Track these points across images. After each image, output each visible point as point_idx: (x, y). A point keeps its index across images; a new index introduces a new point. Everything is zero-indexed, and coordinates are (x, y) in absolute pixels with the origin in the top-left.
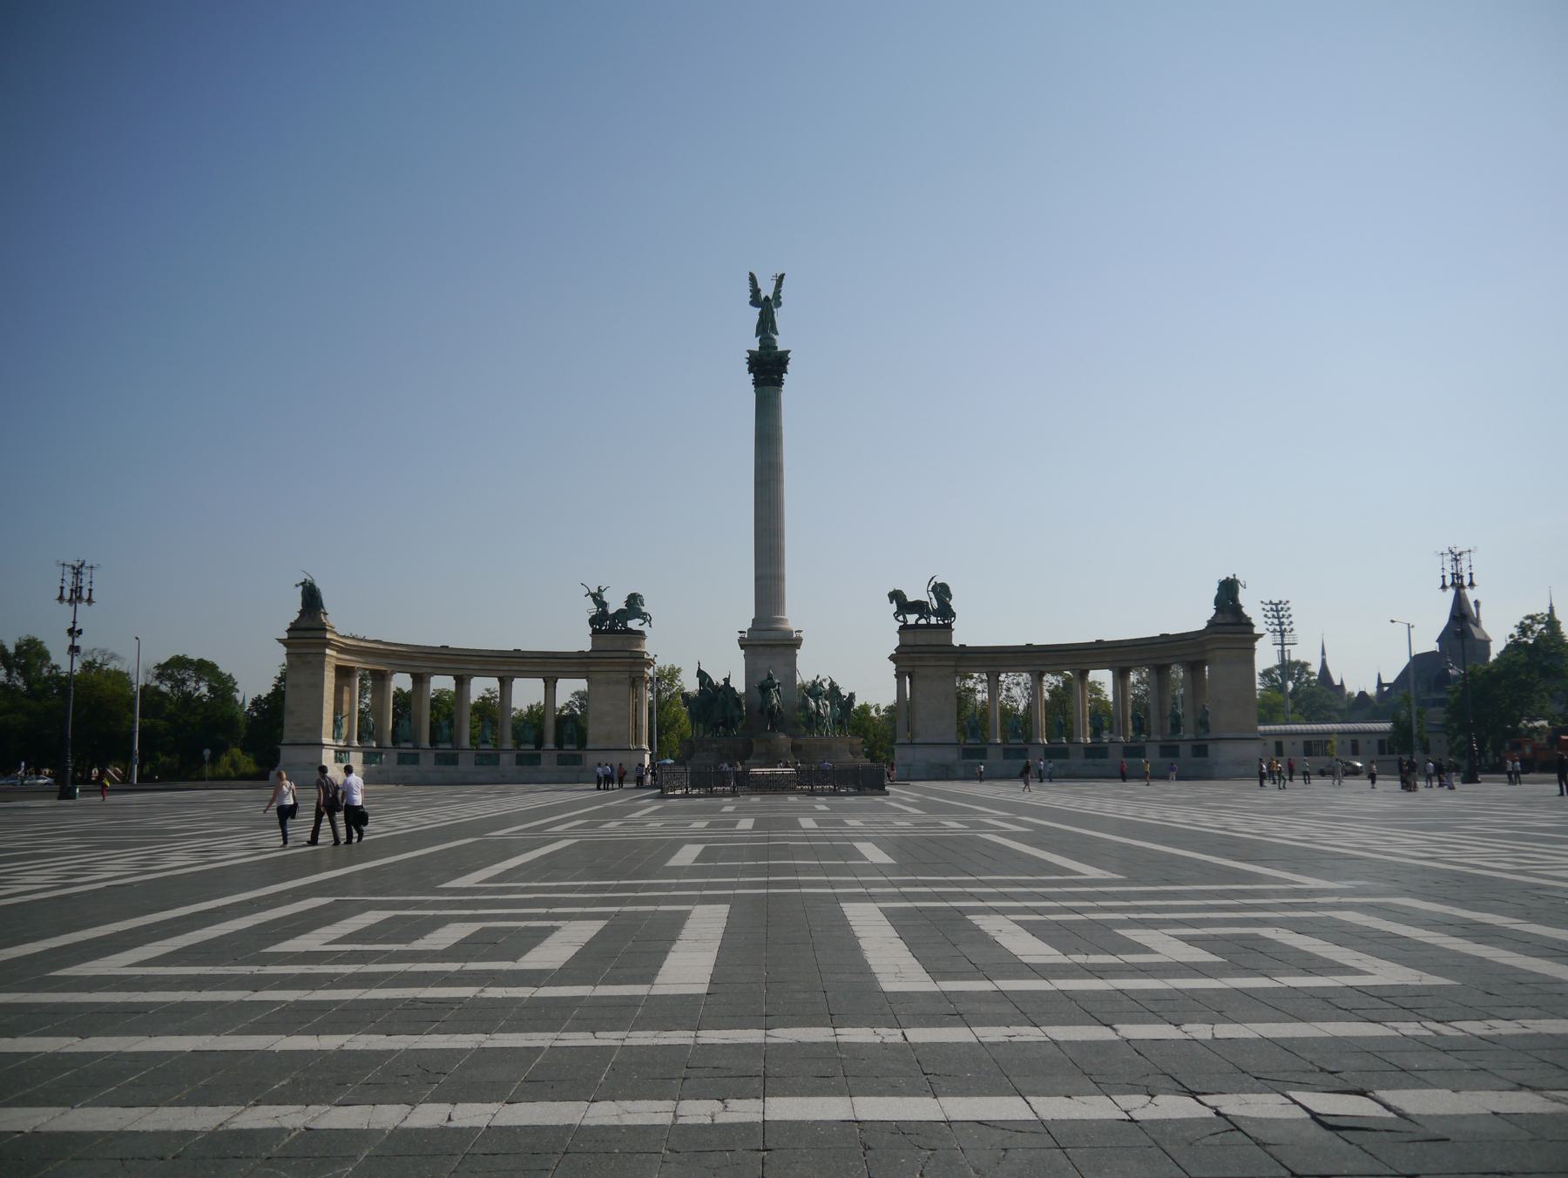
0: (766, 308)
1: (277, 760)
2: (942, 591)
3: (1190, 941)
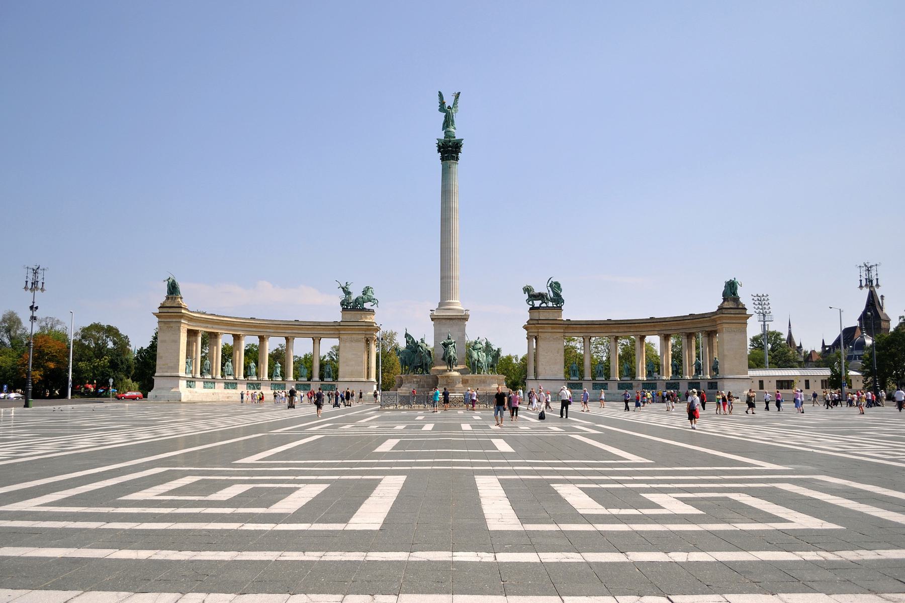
2: (555, 287)
3: (685, 501)
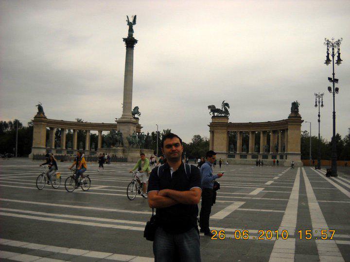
0: (131, 25)
1: (30, 152)
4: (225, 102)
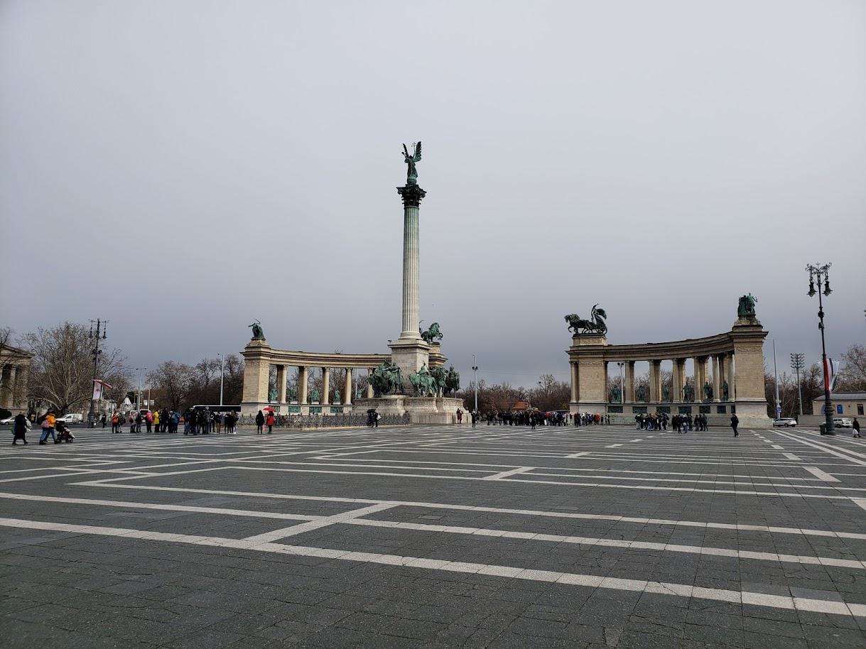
0: (411, 162)
4: (597, 308)
